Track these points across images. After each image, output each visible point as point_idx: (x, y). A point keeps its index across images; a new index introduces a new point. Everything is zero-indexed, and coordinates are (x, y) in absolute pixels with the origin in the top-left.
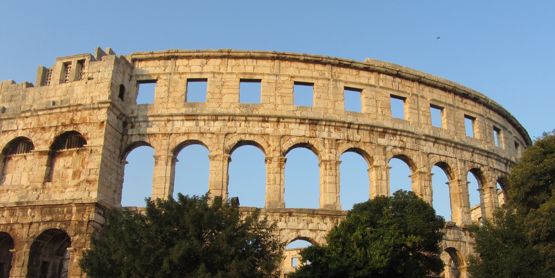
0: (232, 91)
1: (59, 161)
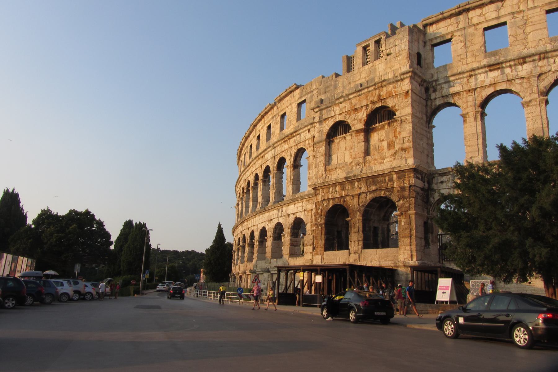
0: (538, 27)
1: (374, 136)
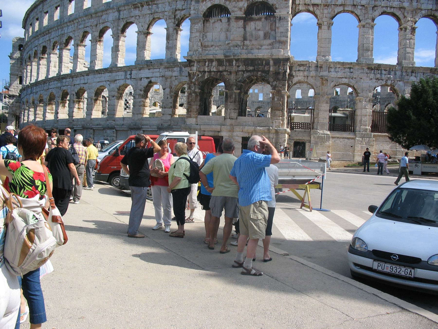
1: (251, 25)
